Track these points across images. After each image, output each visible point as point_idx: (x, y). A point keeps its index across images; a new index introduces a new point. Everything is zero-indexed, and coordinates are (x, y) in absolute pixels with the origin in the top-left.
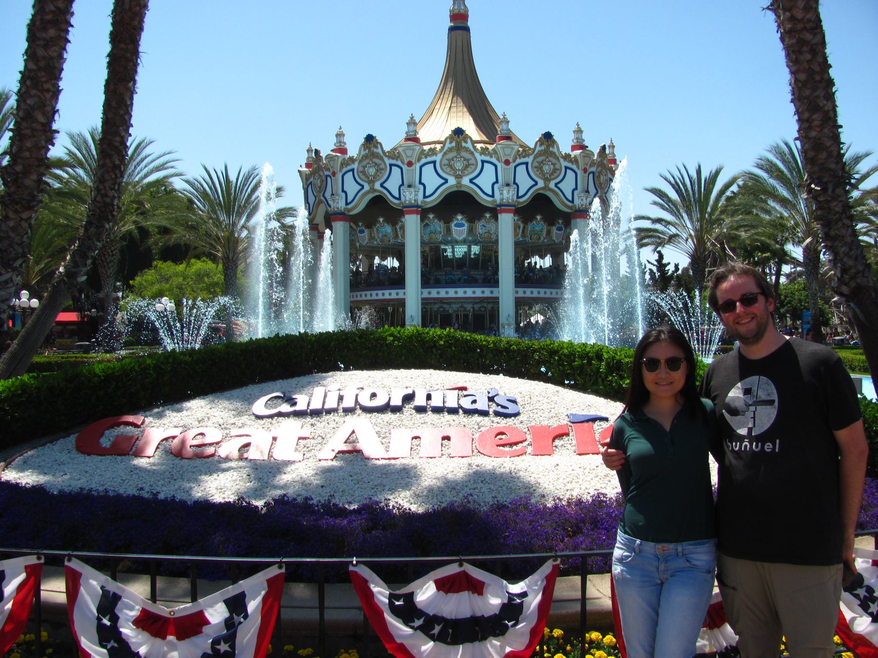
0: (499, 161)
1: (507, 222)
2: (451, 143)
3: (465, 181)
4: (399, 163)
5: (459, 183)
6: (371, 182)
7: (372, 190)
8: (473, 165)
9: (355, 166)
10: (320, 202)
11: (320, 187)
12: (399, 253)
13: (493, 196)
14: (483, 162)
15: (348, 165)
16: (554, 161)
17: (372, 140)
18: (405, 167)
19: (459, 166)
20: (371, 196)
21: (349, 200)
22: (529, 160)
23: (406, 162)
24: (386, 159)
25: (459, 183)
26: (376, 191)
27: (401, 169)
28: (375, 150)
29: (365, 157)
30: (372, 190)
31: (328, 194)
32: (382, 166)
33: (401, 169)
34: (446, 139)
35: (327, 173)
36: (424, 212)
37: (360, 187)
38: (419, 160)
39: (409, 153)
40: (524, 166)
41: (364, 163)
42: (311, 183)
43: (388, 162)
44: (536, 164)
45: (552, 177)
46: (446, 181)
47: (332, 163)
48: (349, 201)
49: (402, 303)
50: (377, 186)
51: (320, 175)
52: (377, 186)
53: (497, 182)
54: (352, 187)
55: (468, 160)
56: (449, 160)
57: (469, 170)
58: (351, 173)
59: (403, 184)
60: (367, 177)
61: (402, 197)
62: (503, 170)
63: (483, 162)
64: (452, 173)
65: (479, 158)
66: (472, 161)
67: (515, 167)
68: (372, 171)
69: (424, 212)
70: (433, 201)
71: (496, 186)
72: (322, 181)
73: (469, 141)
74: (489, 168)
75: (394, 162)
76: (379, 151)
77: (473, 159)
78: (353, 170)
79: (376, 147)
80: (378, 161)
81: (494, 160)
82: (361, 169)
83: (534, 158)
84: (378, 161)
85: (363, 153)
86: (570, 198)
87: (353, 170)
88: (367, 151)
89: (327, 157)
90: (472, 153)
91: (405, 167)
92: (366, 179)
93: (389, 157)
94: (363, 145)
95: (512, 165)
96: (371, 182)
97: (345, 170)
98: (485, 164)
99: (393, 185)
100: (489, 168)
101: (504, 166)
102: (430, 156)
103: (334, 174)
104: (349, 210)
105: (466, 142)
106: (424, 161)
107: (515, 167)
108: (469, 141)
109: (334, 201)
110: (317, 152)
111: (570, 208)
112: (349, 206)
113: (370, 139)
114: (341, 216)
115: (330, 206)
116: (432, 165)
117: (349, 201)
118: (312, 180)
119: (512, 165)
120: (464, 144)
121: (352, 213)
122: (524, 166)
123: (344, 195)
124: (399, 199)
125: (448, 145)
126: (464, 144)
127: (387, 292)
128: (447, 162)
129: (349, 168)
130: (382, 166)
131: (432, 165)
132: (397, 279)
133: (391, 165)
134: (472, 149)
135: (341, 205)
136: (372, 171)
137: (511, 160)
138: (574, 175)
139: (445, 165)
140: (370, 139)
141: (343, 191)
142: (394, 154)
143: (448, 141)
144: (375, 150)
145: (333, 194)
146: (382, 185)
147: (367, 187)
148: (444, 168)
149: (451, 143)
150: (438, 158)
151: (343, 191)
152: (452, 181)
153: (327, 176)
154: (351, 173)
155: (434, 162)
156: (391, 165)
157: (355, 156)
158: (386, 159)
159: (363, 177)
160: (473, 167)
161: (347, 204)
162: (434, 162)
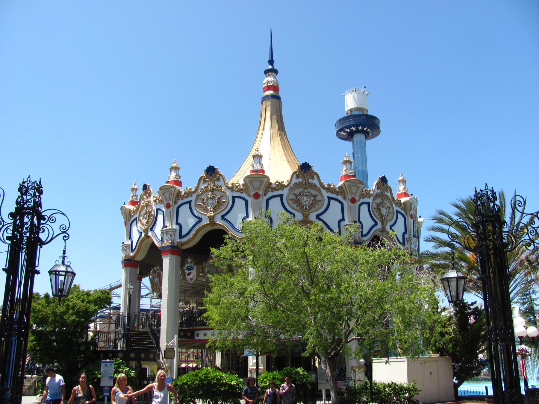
0: (345, 199)
8: (319, 201)
14: (330, 198)
17: (214, 172)
19: (306, 200)
21: (183, 233)
27: (246, 201)
33: (246, 201)
38: (265, 195)
48: (183, 234)
53: (343, 219)
55: (315, 196)
58: (188, 205)
62: (350, 208)
63: (330, 198)
64: (298, 208)
65: (326, 194)
66: (319, 198)
67: (360, 205)
71: (342, 223)
78: (190, 202)
81: (340, 198)
87: (190, 202)
90: (319, 189)
95: (358, 203)
98: (332, 201)
101: (350, 204)
102: (277, 190)
104: (182, 244)
106: (270, 194)
107: (360, 205)
112: (184, 240)
113: (211, 171)
116: (279, 199)
117: (183, 234)
119: (358, 203)
120: (310, 181)
126: (310, 181)
131: (279, 198)
134: (319, 186)
137: (357, 198)
139: (292, 200)
140: (211, 171)
141: (177, 223)
148: (291, 202)
154: (188, 205)
160: (320, 203)
161: (181, 237)
162: (281, 196)
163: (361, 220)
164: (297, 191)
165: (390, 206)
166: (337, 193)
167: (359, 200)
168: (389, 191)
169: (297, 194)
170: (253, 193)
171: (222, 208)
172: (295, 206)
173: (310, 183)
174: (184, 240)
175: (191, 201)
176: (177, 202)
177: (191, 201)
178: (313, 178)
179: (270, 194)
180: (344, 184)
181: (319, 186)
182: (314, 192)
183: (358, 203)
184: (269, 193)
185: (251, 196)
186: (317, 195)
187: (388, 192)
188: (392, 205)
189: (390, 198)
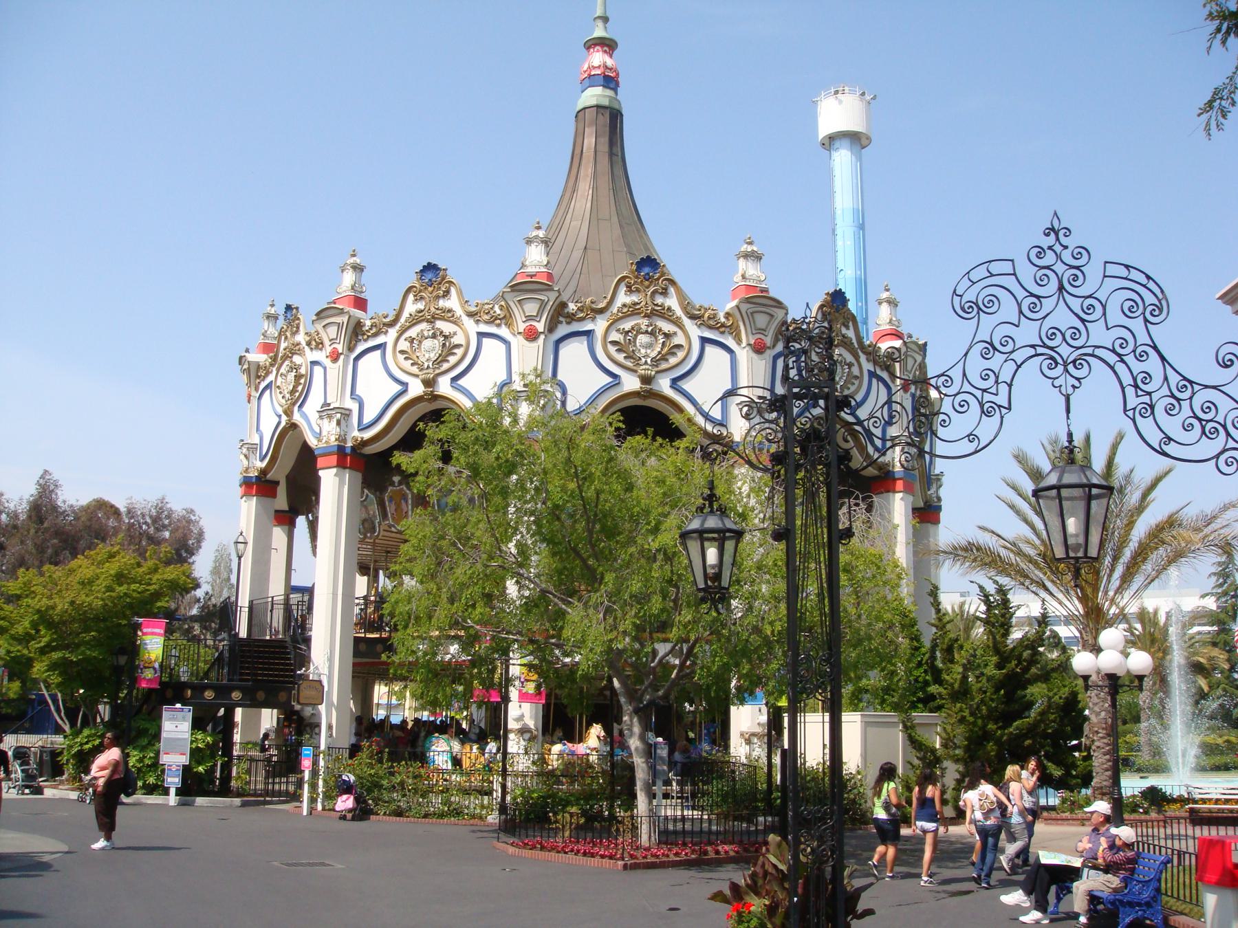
0: (739, 342)
3: (664, 385)
14: (704, 341)
21: (368, 418)
37: (399, 388)
41: (413, 332)
55: (667, 336)
57: (673, 361)
58: (378, 353)
64: (629, 364)
65: (695, 331)
68: (430, 349)
77: (680, 332)
78: (382, 347)
92: (415, 370)
104: (365, 443)
121: (369, 450)
126: (659, 300)
148: (612, 349)
152: (631, 383)
153: (314, 363)
156: (481, 335)
162: (588, 333)
164: (627, 325)
165: (853, 361)
166: (720, 328)
167: (774, 346)
168: (851, 324)
169: (626, 329)
170: (522, 327)
171: (453, 360)
172: (620, 357)
173: (657, 305)
174: (368, 435)
175: (386, 343)
176: (355, 346)
177: (386, 343)
179: (563, 330)
180: (737, 307)
181: (679, 312)
182: (666, 327)
184: (560, 326)
185: (519, 333)
186: (675, 333)
187: (847, 328)
188: (857, 358)
189: (854, 341)
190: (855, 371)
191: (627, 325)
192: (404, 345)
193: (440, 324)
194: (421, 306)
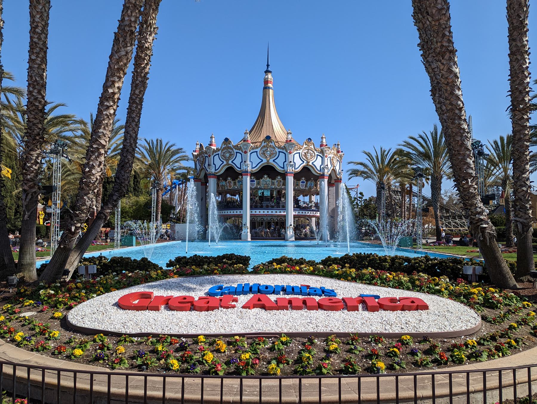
1: (290, 179)
2: (265, 143)
3: (271, 161)
4: (240, 152)
5: (268, 161)
6: (227, 160)
7: (228, 164)
9: (220, 152)
10: (203, 169)
11: (202, 162)
12: (240, 192)
13: (283, 168)
14: (279, 152)
15: (216, 152)
16: (312, 152)
18: (243, 154)
20: (227, 167)
22: (301, 151)
23: (244, 151)
24: (234, 149)
25: (268, 161)
26: (229, 164)
27: (241, 154)
28: (229, 145)
29: (224, 148)
30: (228, 164)
31: (206, 165)
32: (232, 153)
33: (241, 154)
34: (263, 141)
35: (206, 155)
36: (252, 174)
39: (245, 147)
40: (298, 154)
41: (224, 151)
42: (198, 160)
43: (235, 151)
44: (303, 154)
45: (311, 160)
46: (262, 161)
47: (208, 150)
49: (241, 216)
50: (230, 162)
51: (203, 157)
52: (230, 162)
53: (286, 161)
54: (218, 162)
56: (264, 151)
59: (242, 162)
60: (225, 158)
61: (242, 168)
63: (279, 152)
68: (228, 155)
69: (252, 174)
70: (255, 170)
71: (285, 163)
72: (203, 159)
73: (273, 142)
74: (282, 155)
75: (238, 151)
76: (231, 145)
78: (218, 154)
79: (230, 144)
80: (230, 151)
81: (284, 151)
82: (222, 154)
83: (303, 150)
84: (230, 151)
85: (223, 146)
86: (319, 169)
88: (225, 146)
89: (206, 148)
91: (243, 154)
93: (236, 149)
94: (224, 142)
96: (227, 160)
97: (215, 154)
99: (237, 161)
100: (282, 155)
103: (209, 156)
105: (272, 143)
107: (294, 155)
108: (273, 142)
109: (209, 168)
110: (201, 145)
111: (320, 174)
112: (217, 171)
113: (226, 140)
114: (214, 175)
115: (207, 171)
118: (198, 158)
121: (217, 174)
122: (298, 154)
123: (214, 165)
124: (240, 168)
125: (263, 144)
127: (235, 211)
128: (262, 152)
129: (217, 153)
130: (232, 153)
132: (240, 206)
133: (237, 153)
135: (213, 170)
136: (228, 155)
138: (321, 158)
140: (226, 140)
141: (214, 164)
142: (236, 147)
143: (263, 142)
144: (229, 145)
145: (209, 165)
146: (232, 162)
147: (225, 163)
149: (265, 143)
150: (258, 150)
151: (214, 164)
152: (265, 161)
153: (206, 157)
155: (257, 152)
156: (237, 153)
157: (219, 148)
158: (234, 149)
159: (223, 158)
161: (216, 170)
162: (257, 152)
163: (295, 161)
178: (272, 143)
183: (294, 153)
190: (313, 155)
191: (264, 149)
192: (222, 154)
193: (229, 150)
194: (225, 146)
